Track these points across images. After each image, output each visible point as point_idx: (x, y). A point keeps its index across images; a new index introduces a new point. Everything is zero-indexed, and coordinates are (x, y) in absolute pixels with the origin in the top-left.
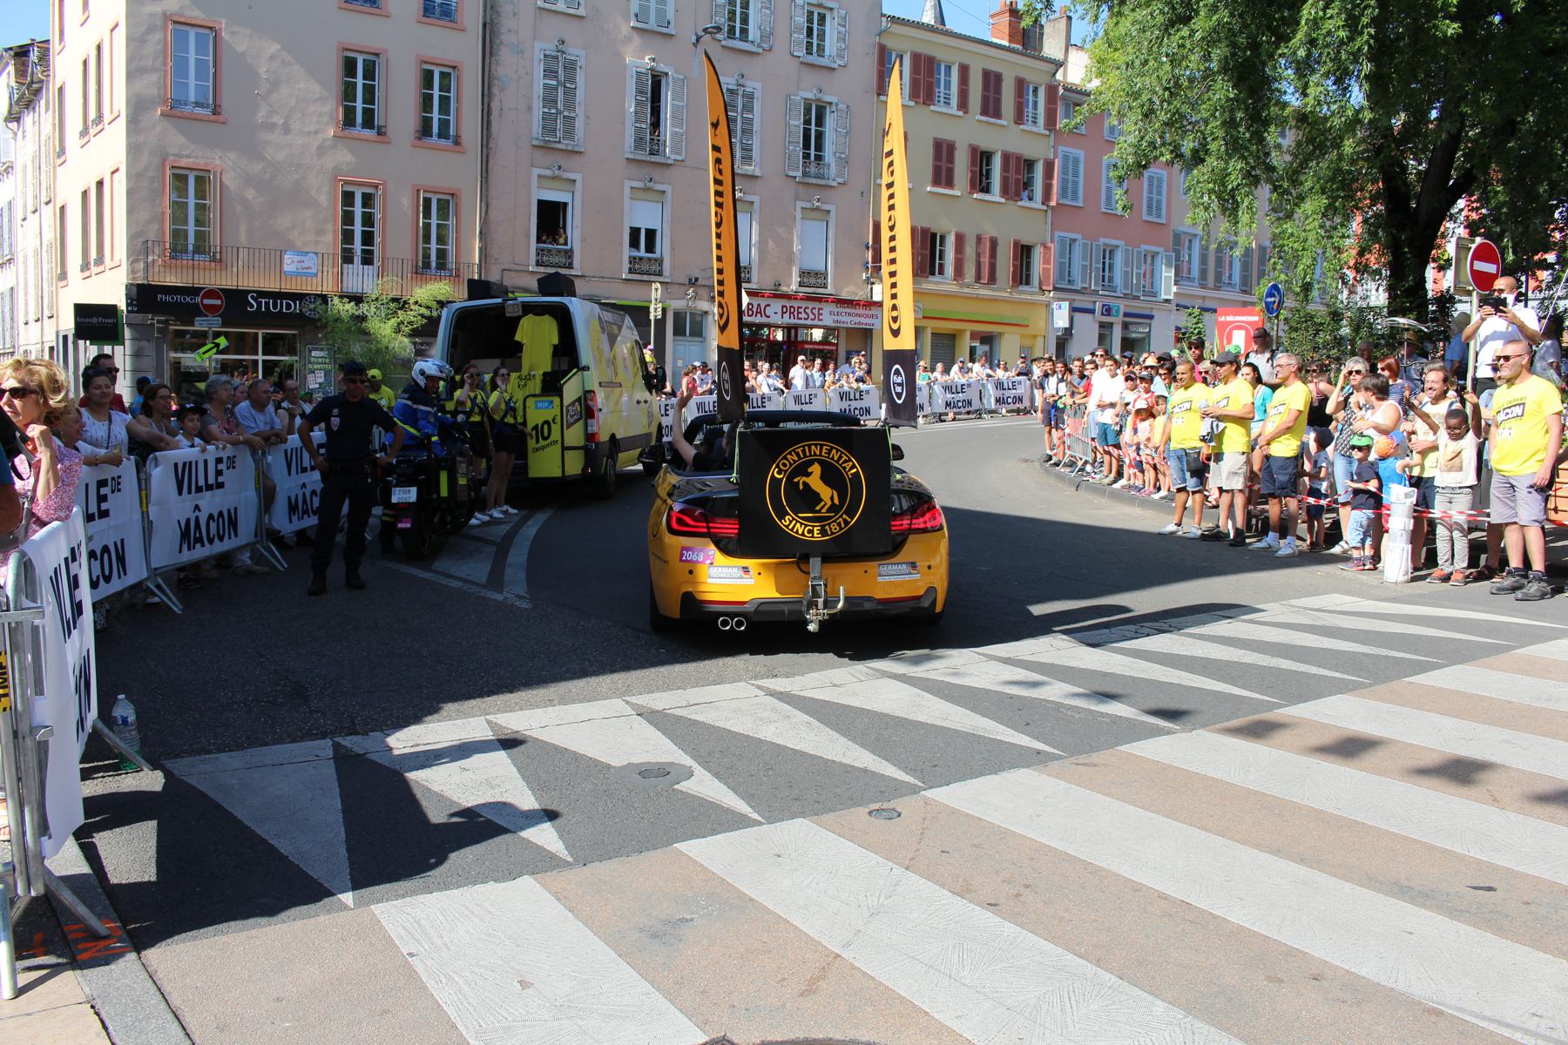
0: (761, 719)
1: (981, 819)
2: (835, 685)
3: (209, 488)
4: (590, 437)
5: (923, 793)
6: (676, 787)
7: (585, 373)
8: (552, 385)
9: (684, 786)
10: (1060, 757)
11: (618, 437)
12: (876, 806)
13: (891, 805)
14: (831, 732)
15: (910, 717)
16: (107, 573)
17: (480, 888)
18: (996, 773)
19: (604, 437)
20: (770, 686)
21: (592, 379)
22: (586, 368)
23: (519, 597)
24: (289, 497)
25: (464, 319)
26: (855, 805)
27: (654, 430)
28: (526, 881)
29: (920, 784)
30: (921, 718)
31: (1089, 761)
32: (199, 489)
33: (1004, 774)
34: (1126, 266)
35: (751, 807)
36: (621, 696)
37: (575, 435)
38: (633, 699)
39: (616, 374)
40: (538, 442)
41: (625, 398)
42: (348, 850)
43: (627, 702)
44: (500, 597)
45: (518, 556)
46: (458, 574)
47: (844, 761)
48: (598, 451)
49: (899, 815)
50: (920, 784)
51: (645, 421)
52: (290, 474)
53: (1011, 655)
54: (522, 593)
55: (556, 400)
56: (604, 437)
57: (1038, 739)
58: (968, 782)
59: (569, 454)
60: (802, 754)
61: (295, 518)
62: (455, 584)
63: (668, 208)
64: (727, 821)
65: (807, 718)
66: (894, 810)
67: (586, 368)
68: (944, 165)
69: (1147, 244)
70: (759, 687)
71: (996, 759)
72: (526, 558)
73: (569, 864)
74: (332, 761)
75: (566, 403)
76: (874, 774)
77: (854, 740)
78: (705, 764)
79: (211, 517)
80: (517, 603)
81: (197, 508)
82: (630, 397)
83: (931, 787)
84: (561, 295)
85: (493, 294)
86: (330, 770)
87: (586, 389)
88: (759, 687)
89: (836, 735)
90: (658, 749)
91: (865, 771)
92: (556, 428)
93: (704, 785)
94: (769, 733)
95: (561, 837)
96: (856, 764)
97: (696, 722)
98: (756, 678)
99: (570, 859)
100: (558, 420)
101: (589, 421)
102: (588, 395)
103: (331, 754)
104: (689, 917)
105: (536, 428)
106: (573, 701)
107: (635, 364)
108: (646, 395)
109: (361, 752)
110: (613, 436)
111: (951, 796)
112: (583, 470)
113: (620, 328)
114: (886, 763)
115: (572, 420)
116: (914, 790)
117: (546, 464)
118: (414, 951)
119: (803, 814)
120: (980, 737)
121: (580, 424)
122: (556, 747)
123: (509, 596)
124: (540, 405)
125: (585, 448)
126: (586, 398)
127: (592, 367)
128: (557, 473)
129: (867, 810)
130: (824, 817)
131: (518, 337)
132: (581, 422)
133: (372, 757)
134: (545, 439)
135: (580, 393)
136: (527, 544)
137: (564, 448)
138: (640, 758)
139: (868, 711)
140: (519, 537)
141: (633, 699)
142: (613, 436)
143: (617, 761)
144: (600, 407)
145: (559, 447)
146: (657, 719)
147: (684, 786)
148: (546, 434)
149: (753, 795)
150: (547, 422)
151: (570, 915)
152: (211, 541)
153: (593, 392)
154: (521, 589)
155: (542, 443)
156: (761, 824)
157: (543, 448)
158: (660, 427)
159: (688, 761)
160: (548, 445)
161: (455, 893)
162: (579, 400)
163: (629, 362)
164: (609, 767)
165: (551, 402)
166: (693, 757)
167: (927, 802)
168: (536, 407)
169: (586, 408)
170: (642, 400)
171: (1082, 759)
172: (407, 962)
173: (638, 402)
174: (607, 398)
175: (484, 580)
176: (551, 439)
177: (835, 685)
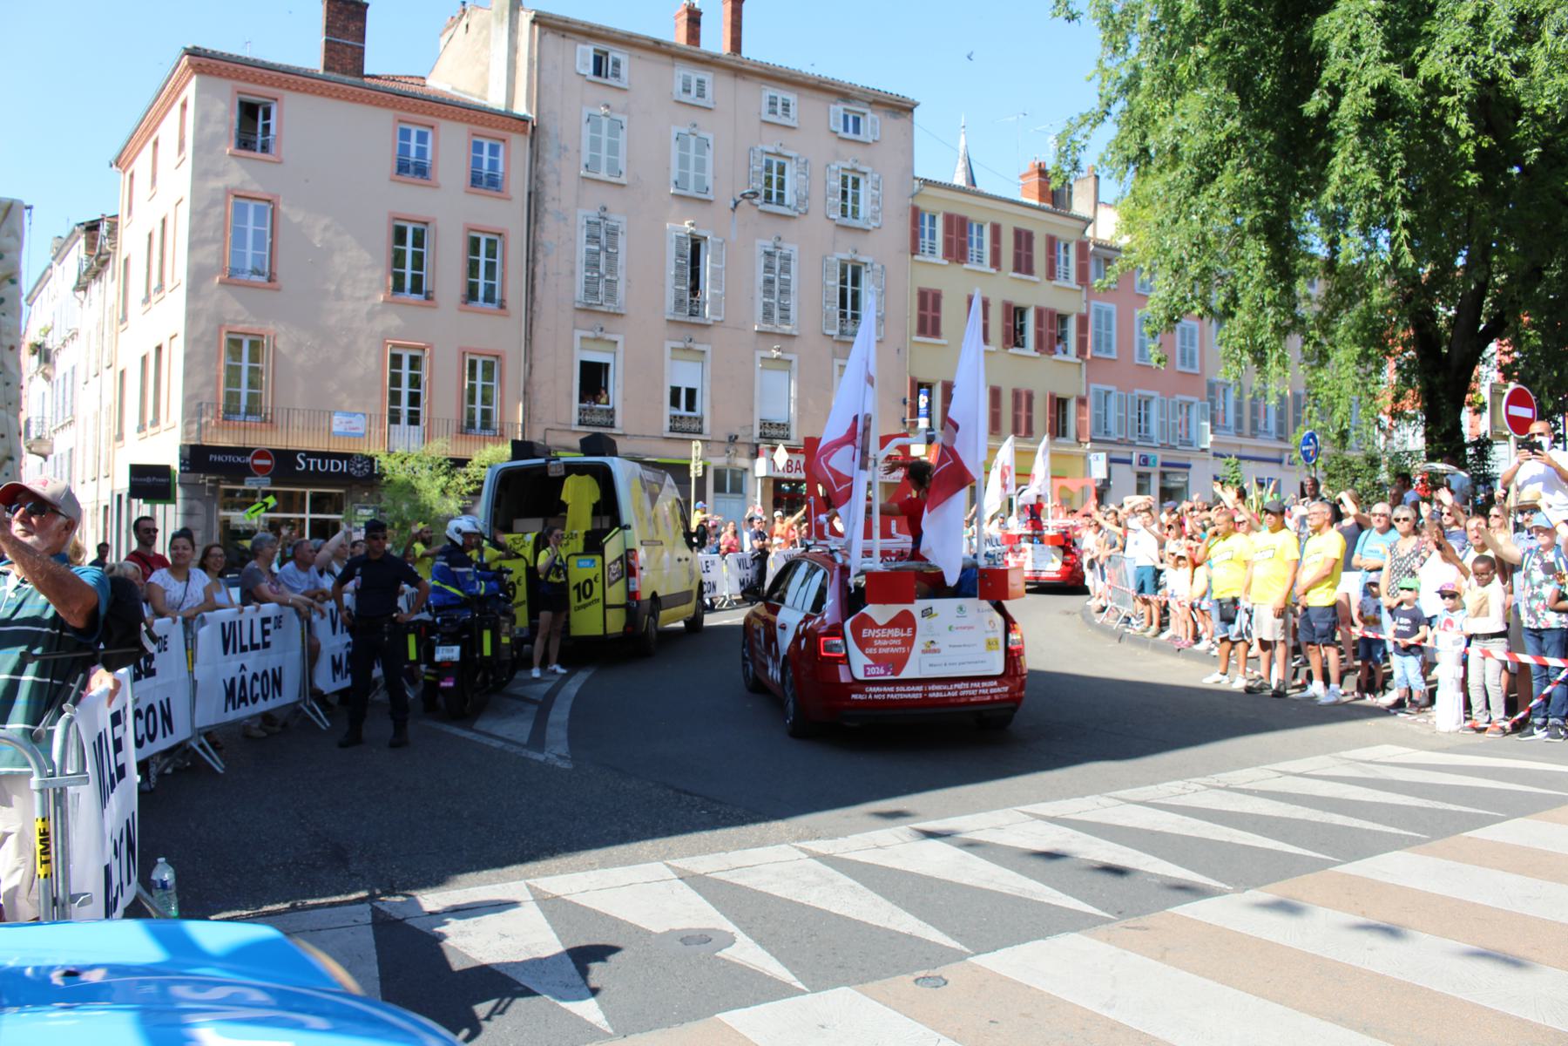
0: (804, 883)
1: (1029, 987)
2: (878, 847)
3: (255, 647)
4: (632, 595)
5: (970, 959)
6: (718, 954)
7: (627, 532)
8: (594, 544)
9: (726, 953)
10: (1108, 921)
11: (660, 594)
12: (922, 973)
14: (875, 896)
15: (956, 879)
16: (151, 732)
18: (1044, 938)
19: (645, 595)
20: (813, 849)
21: (634, 537)
22: (627, 527)
23: (560, 757)
24: (333, 657)
25: (507, 481)
27: (695, 588)
29: (967, 950)
30: (966, 881)
31: (1139, 924)
32: (244, 649)
33: (1051, 939)
34: (1120, 410)
35: (795, 975)
36: (664, 858)
37: (616, 594)
38: (674, 863)
39: (657, 532)
40: (579, 600)
41: (666, 555)
43: (669, 866)
44: (541, 757)
45: (560, 715)
46: (500, 734)
47: (890, 926)
48: (640, 610)
49: (946, 983)
50: (967, 950)
51: (686, 578)
52: (334, 632)
53: (1058, 814)
54: (564, 753)
55: (598, 559)
56: (645, 595)
57: (1085, 901)
58: (1016, 947)
59: (610, 613)
60: (847, 919)
61: (338, 677)
62: (496, 744)
64: (772, 990)
65: (851, 882)
66: (940, 977)
67: (627, 527)
68: (929, 313)
69: (1140, 387)
70: (801, 850)
71: (1046, 923)
72: (567, 716)
73: (609, 1035)
75: (608, 561)
76: (920, 940)
77: (898, 904)
78: (748, 931)
79: (255, 676)
80: (559, 764)
81: (243, 667)
82: (671, 555)
83: (978, 953)
84: (603, 454)
85: (536, 453)
86: (367, 937)
87: (628, 547)
88: (801, 850)
89: (880, 899)
90: (700, 914)
91: (910, 937)
92: (597, 587)
93: (747, 952)
94: (813, 898)
96: (901, 930)
97: (740, 886)
98: (799, 839)
99: (610, 1030)
100: (600, 578)
101: (631, 579)
102: (630, 555)
103: (369, 919)
105: (577, 587)
106: (614, 865)
107: (676, 521)
108: (687, 552)
110: (654, 594)
111: (1002, 962)
112: (625, 628)
113: (661, 487)
114: (931, 928)
115: (613, 579)
116: (960, 956)
117: (588, 622)
119: (847, 982)
120: (1027, 900)
121: (622, 581)
122: (596, 913)
123: (551, 756)
124: (582, 563)
125: (626, 606)
126: (629, 554)
127: (634, 525)
128: (600, 632)
129: (913, 978)
130: (870, 986)
131: (563, 497)
132: (622, 581)
133: (410, 922)
134: (587, 597)
135: (622, 552)
136: (568, 703)
137: (606, 607)
138: (681, 924)
139: (912, 874)
140: (559, 698)
141: (674, 863)
142: (654, 594)
143: (657, 928)
144: (641, 564)
145: (600, 606)
146: (699, 883)
147: (726, 953)
148: (588, 592)
149: (796, 963)
150: (589, 581)
152: (255, 700)
153: (634, 550)
154: (562, 749)
155: (584, 601)
156: (803, 993)
157: (585, 606)
158: (701, 584)
159: (729, 926)
160: (590, 604)
162: (620, 558)
163: (670, 520)
164: (649, 933)
165: (593, 561)
166: (736, 923)
167: (976, 969)
168: (579, 566)
169: (628, 568)
170: (683, 557)
171: (1132, 922)
173: (679, 560)
174: (648, 556)
175: (525, 740)
176: (593, 598)
177: (878, 847)
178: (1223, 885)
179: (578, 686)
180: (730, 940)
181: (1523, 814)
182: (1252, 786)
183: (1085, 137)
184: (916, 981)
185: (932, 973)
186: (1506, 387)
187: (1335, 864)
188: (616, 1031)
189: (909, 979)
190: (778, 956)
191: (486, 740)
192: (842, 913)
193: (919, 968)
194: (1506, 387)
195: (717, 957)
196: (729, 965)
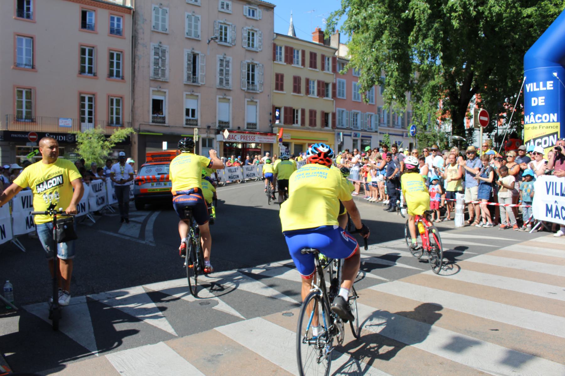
6: (213, 308)
9: (216, 307)
12: (285, 312)
13: (290, 311)
15: (295, 280)
17: (145, 347)
23: (151, 242)
26: (277, 312)
28: (161, 344)
35: (241, 314)
42: (95, 335)
44: (144, 242)
45: (150, 227)
54: (152, 241)
62: (127, 238)
63: (231, 105)
64: (232, 319)
66: (291, 313)
72: (152, 228)
73: (176, 337)
74: (86, 304)
80: (151, 244)
86: (85, 307)
95: (173, 327)
99: (177, 335)
103: (85, 301)
104: (221, 354)
109: (97, 300)
118: (122, 371)
119: (259, 316)
123: (147, 242)
129: (282, 313)
133: (100, 301)
136: (153, 223)
140: (149, 221)
147: (216, 307)
149: (241, 310)
151: (178, 355)
154: (152, 239)
156: (244, 320)
161: (135, 349)
172: (120, 375)
175: (137, 236)
178: (385, 279)
179: (156, 217)
180: (217, 303)
181: (483, 253)
182: (395, 246)
183: (337, 20)
184: (283, 314)
185: (288, 311)
186: (479, 110)
187: (423, 271)
188: (179, 335)
189: (280, 314)
190: (234, 308)
191: (123, 237)
192: (256, 292)
193: (283, 310)
194: (479, 110)
195: (213, 309)
196: (217, 311)
